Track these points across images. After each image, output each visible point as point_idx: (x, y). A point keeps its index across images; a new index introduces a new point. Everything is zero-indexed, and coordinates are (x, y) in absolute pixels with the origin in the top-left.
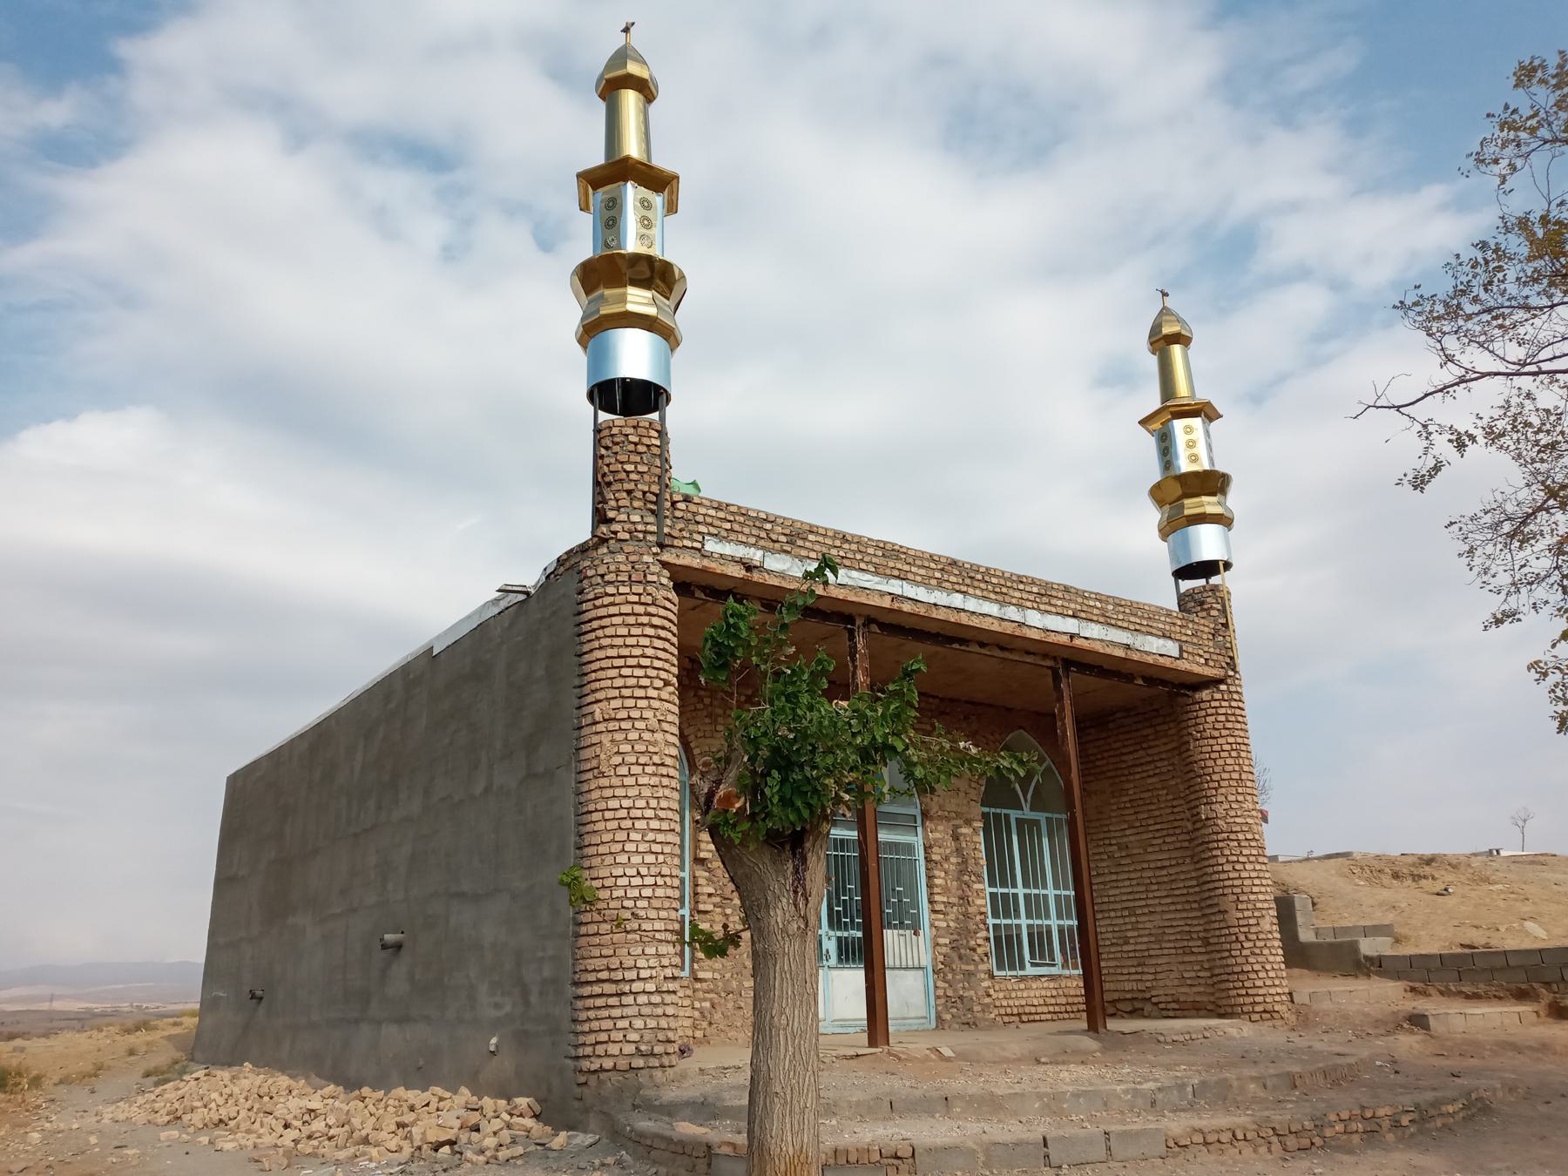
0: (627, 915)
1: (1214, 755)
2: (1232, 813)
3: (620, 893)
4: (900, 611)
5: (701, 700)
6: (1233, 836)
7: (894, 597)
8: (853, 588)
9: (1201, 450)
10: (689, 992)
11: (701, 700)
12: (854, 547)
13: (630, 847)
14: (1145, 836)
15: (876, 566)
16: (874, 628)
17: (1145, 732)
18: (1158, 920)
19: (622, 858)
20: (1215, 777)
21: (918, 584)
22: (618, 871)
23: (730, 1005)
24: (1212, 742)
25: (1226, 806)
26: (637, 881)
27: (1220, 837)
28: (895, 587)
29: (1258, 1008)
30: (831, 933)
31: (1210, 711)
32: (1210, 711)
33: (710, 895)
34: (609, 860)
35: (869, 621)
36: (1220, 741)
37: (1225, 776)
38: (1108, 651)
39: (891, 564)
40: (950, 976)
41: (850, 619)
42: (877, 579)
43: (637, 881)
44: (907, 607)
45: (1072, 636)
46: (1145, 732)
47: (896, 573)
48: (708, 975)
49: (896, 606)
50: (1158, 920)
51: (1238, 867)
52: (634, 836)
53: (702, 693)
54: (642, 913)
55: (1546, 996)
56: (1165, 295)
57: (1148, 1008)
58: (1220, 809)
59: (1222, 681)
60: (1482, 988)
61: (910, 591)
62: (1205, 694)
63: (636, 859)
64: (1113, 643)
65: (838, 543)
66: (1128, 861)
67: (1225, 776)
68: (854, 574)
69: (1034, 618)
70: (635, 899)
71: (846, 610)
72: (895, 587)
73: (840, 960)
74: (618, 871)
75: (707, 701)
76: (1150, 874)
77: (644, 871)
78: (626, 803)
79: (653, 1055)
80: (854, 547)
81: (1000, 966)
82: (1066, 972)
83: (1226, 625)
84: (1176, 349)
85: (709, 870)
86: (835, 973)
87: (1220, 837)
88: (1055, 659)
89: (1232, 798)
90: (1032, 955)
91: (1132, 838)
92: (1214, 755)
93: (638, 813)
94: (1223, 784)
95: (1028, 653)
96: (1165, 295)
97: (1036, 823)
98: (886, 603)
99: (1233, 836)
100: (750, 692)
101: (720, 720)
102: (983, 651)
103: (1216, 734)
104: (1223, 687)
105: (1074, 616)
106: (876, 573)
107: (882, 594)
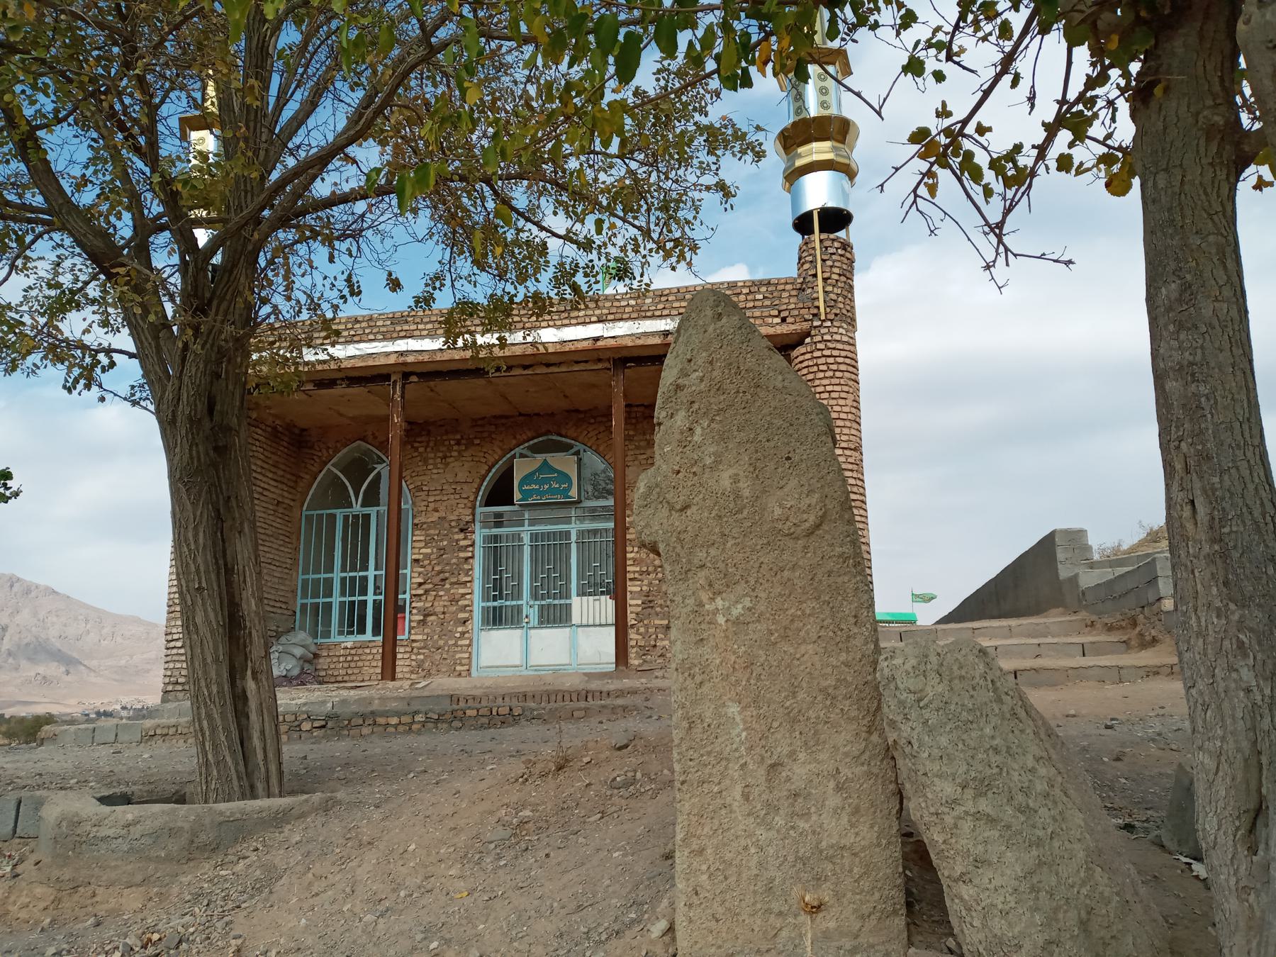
4: (405, 364)
5: (416, 449)
7: (401, 354)
8: (362, 356)
10: (409, 649)
11: (416, 449)
12: (364, 325)
15: (383, 333)
16: (414, 379)
21: (422, 337)
23: (438, 657)
28: (401, 345)
30: (531, 603)
33: (420, 584)
35: (406, 376)
38: (640, 342)
39: (398, 328)
40: (642, 630)
41: (387, 377)
42: (382, 344)
44: (410, 359)
45: (596, 339)
47: (402, 334)
48: (420, 637)
49: (401, 360)
53: (416, 445)
59: (808, 334)
61: (413, 344)
64: (646, 334)
65: (350, 326)
68: (362, 345)
69: (549, 335)
71: (384, 371)
72: (401, 345)
73: (541, 622)
75: (421, 450)
79: (177, 683)
80: (364, 325)
85: (422, 566)
86: (533, 631)
88: (608, 360)
95: (577, 362)
98: (392, 360)
100: (458, 437)
101: (431, 461)
102: (526, 372)
104: (808, 340)
105: (599, 321)
106: (384, 339)
107: (388, 354)
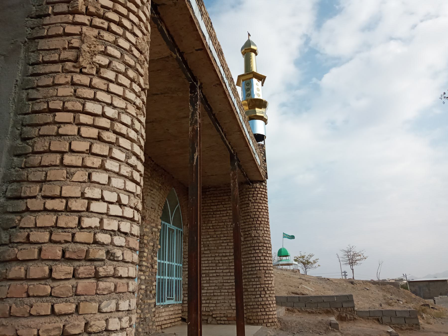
0: (101, 253)
1: (260, 210)
2: (265, 235)
3: (93, 222)
6: (265, 245)
9: (260, 93)
13: (110, 165)
14: (218, 242)
17: (224, 198)
18: (220, 279)
19: (100, 177)
20: (260, 219)
22: (94, 193)
24: (259, 205)
25: (263, 232)
26: (115, 210)
27: (260, 245)
29: (270, 321)
31: (259, 192)
32: (259, 192)
34: (80, 175)
36: (263, 205)
37: (263, 219)
43: (115, 210)
46: (224, 198)
50: (220, 279)
51: (267, 258)
52: (117, 153)
54: (118, 253)
55: (337, 313)
56: (249, 35)
57: (210, 319)
58: (261, 233)
60: (314, 310)
62: (258, 185)
63: (117, 182)
66: (208, 252)
67: (263, 219)
70: (112, 233)
74: (94, 193)
76: (220, 258)
77: (125, 199)
78: (110, 112)
81: (159, 301)
82: (175, 303)
83: (265, 160)
84: (253, 54)
87: (260, 245)
89: (265, 229)
90: (168, 296)
91: (211, 242)
92: (260, 210)
93: (124, 130)
94: (263, 222)
96: (249, 35)
97: (173, 231)
99: (265, 245)
103: (261, 202)
